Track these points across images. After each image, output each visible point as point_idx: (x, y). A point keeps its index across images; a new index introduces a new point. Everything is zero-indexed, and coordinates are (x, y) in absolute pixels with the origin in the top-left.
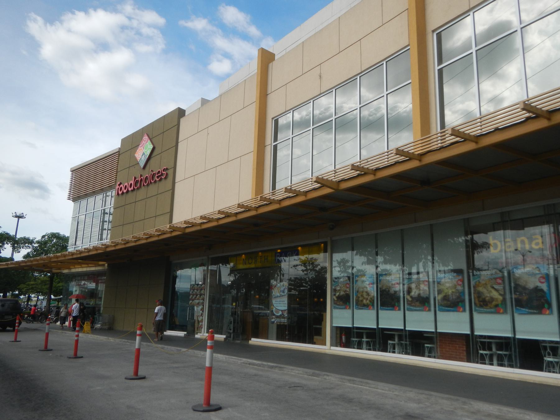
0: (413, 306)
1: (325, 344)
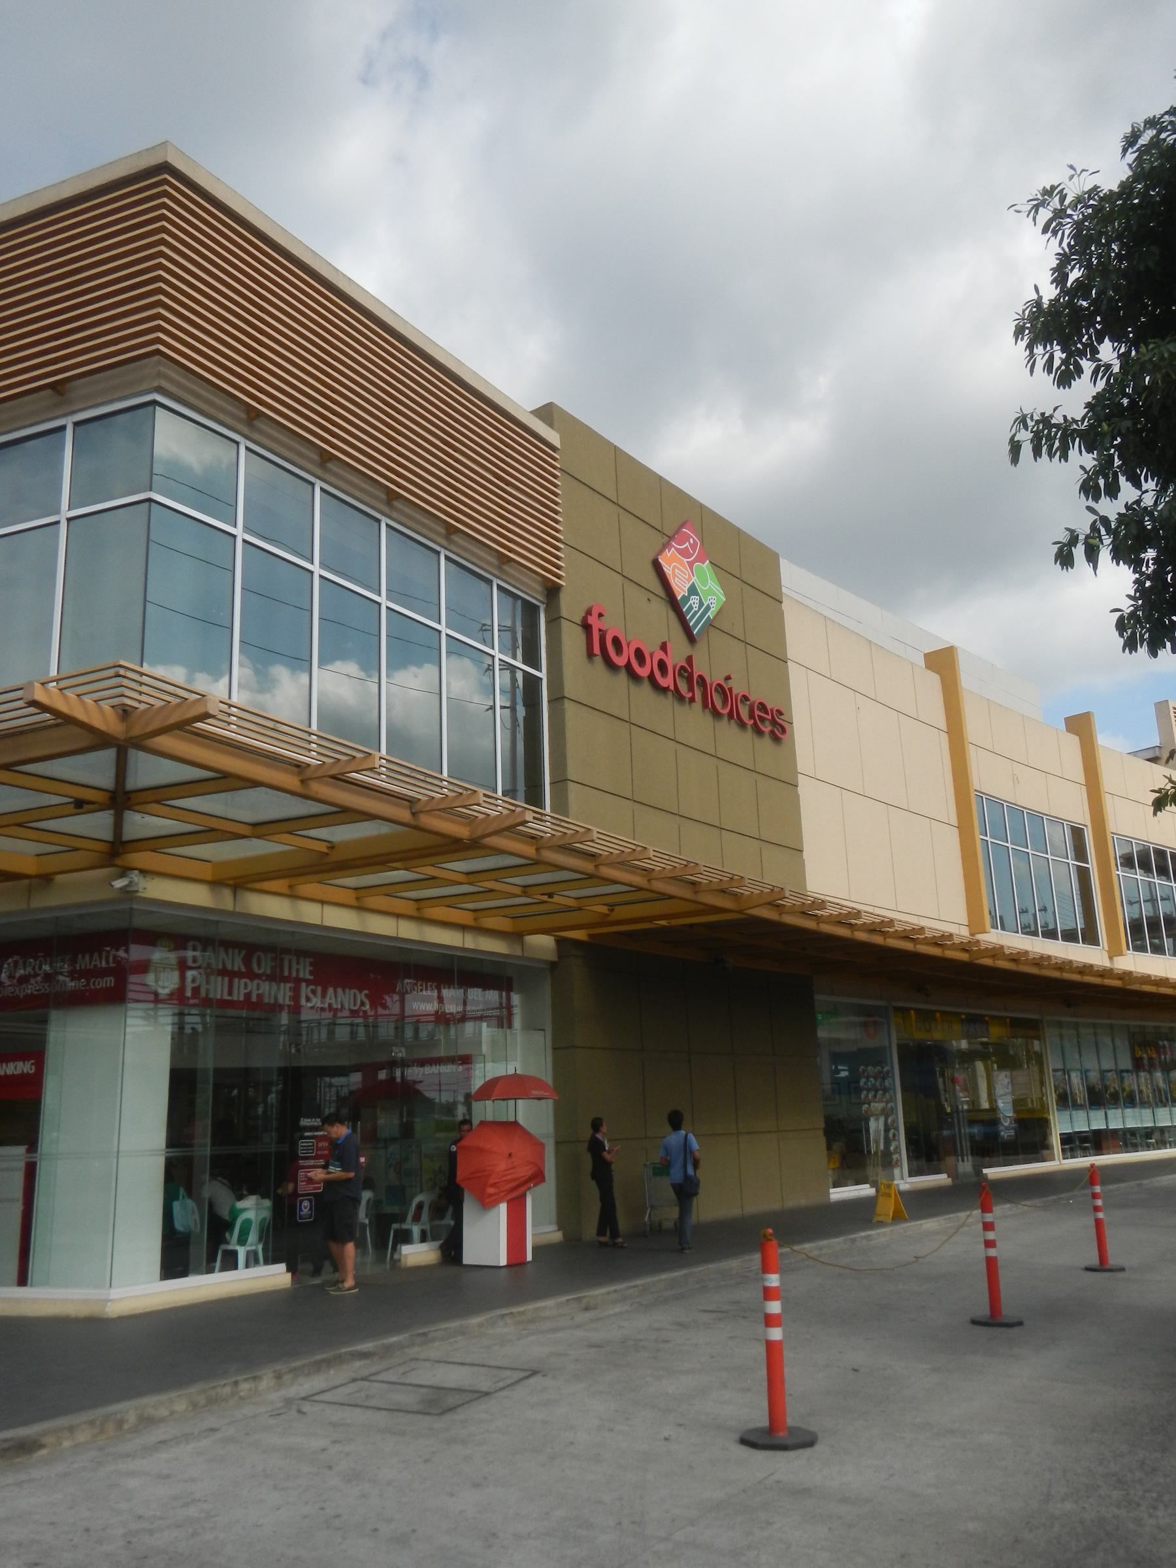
1: (1053, 1159)
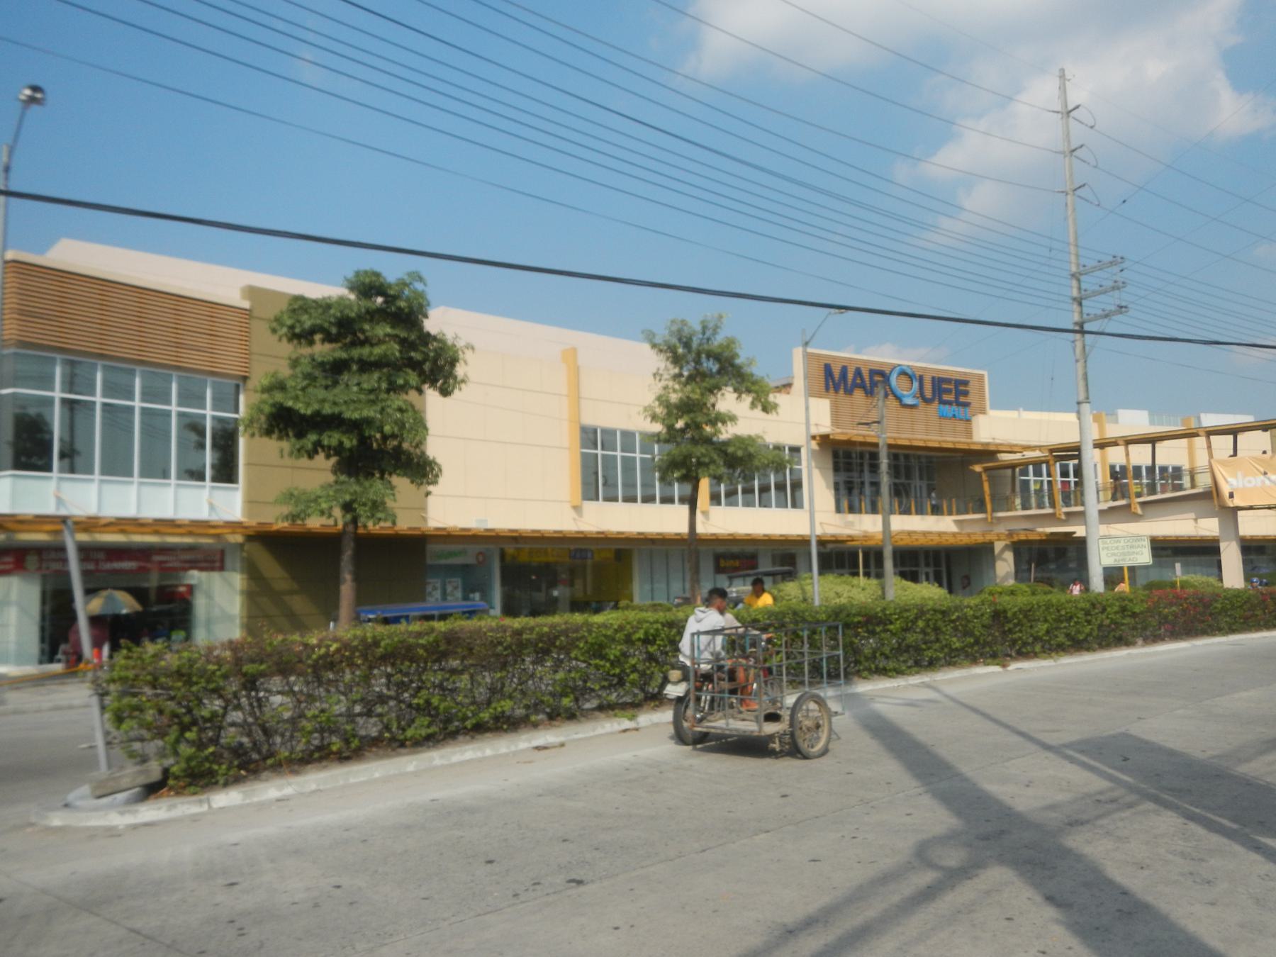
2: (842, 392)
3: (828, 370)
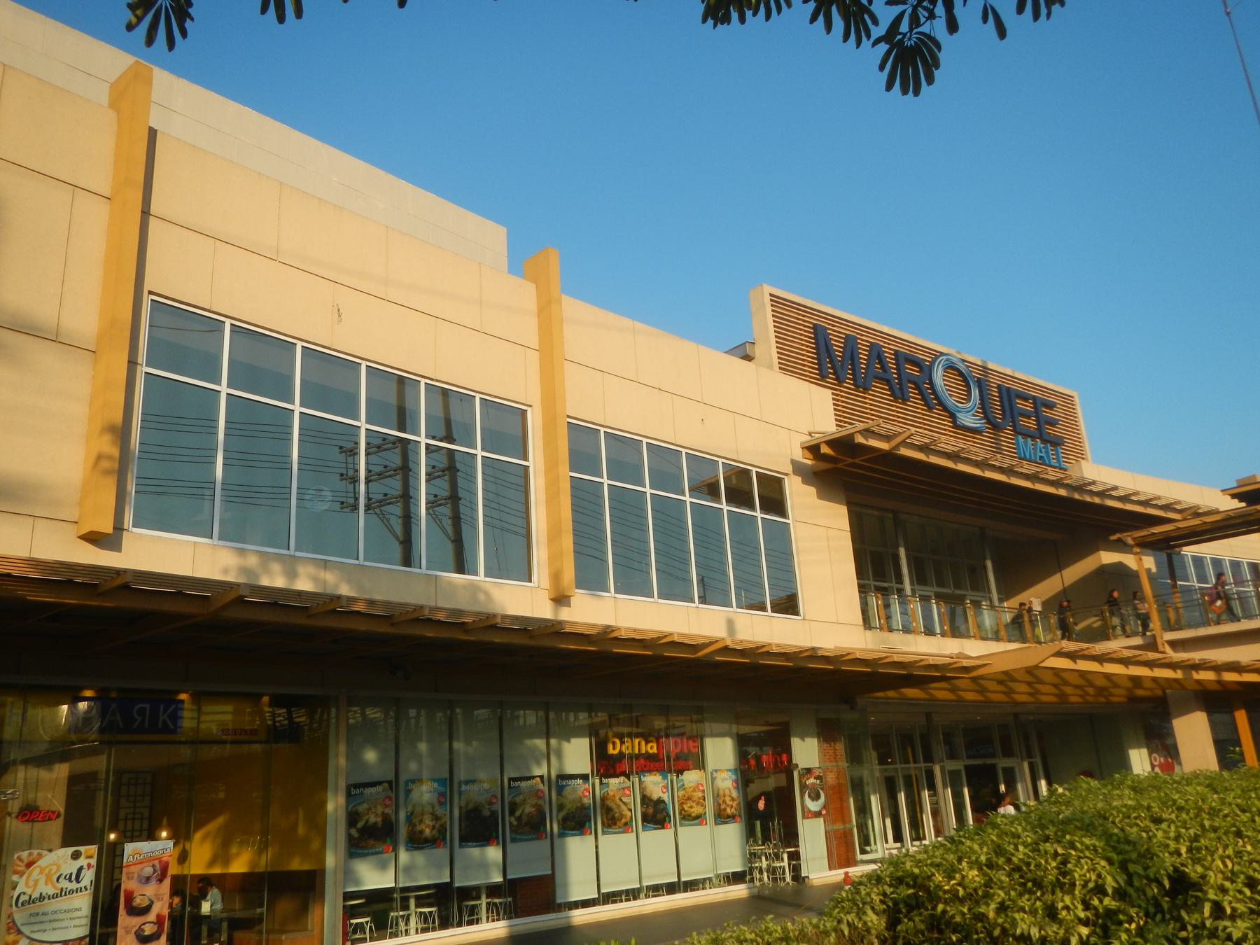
0: (521, 834)
2: (849, 384)
3: (820, 336)
